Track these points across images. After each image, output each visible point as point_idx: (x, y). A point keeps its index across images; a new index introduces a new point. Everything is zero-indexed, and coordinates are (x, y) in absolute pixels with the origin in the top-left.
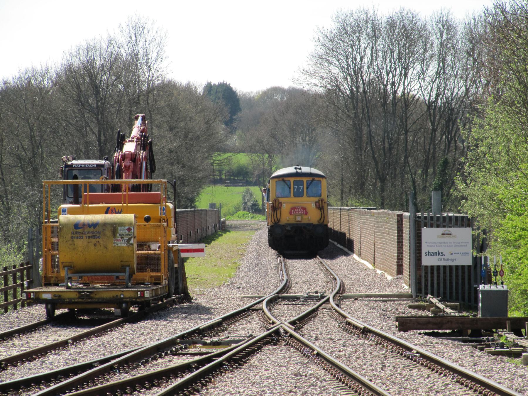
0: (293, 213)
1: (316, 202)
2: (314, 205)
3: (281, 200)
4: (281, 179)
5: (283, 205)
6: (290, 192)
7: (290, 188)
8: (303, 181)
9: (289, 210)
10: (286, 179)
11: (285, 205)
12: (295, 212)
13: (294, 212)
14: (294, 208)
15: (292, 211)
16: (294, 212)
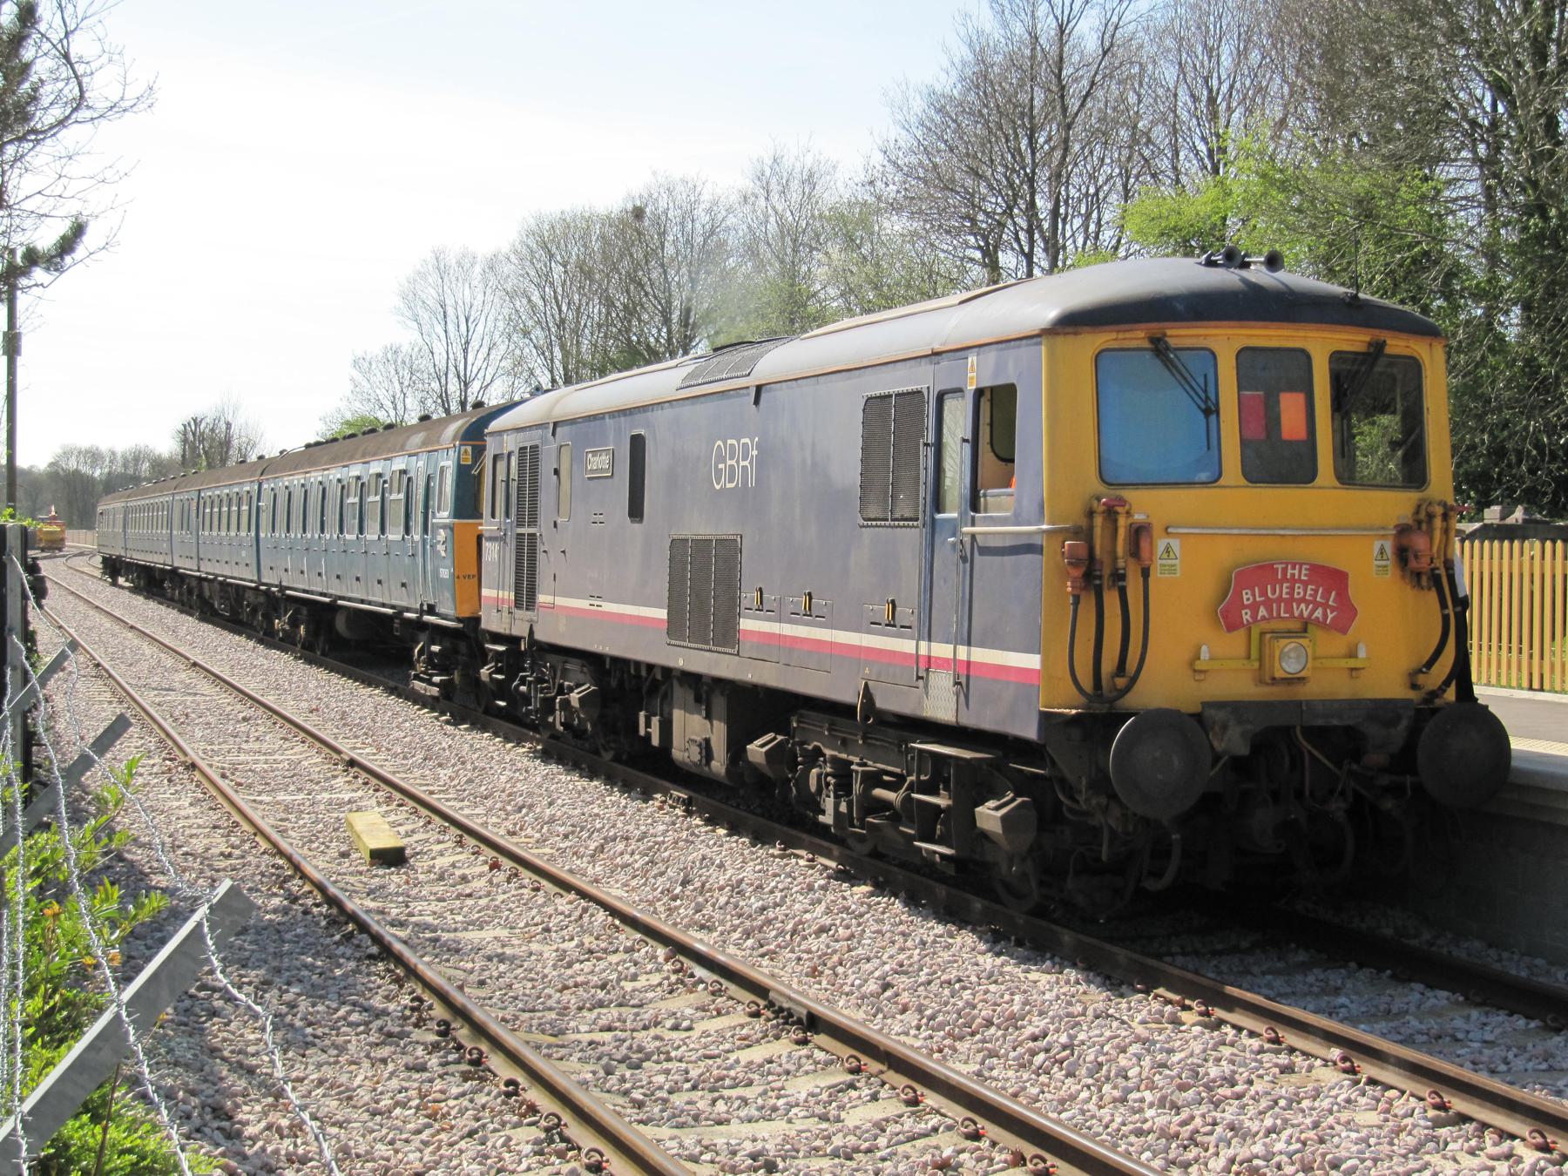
0: (1246, 616)
1: (1403, 530)
2: (1389, 546)
3: (1144, 505)
4: (1137, 336)
5: (1161, 545)
6: (1212, 441)
7: (1211, 410)
8: (1305, 356)
9: (1205, 588)
10: (1181, 335)
11: (1175, 544)
12: (1268, 604)
13: (1254, 607)
14: (1261, 573)
15: (1247, 596)
16: (1254, 607)
